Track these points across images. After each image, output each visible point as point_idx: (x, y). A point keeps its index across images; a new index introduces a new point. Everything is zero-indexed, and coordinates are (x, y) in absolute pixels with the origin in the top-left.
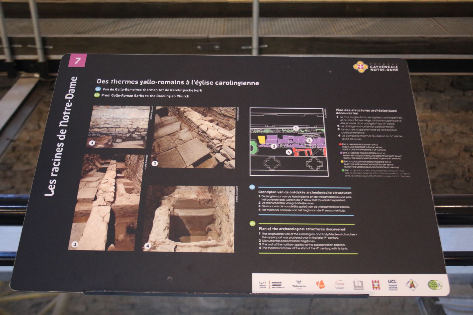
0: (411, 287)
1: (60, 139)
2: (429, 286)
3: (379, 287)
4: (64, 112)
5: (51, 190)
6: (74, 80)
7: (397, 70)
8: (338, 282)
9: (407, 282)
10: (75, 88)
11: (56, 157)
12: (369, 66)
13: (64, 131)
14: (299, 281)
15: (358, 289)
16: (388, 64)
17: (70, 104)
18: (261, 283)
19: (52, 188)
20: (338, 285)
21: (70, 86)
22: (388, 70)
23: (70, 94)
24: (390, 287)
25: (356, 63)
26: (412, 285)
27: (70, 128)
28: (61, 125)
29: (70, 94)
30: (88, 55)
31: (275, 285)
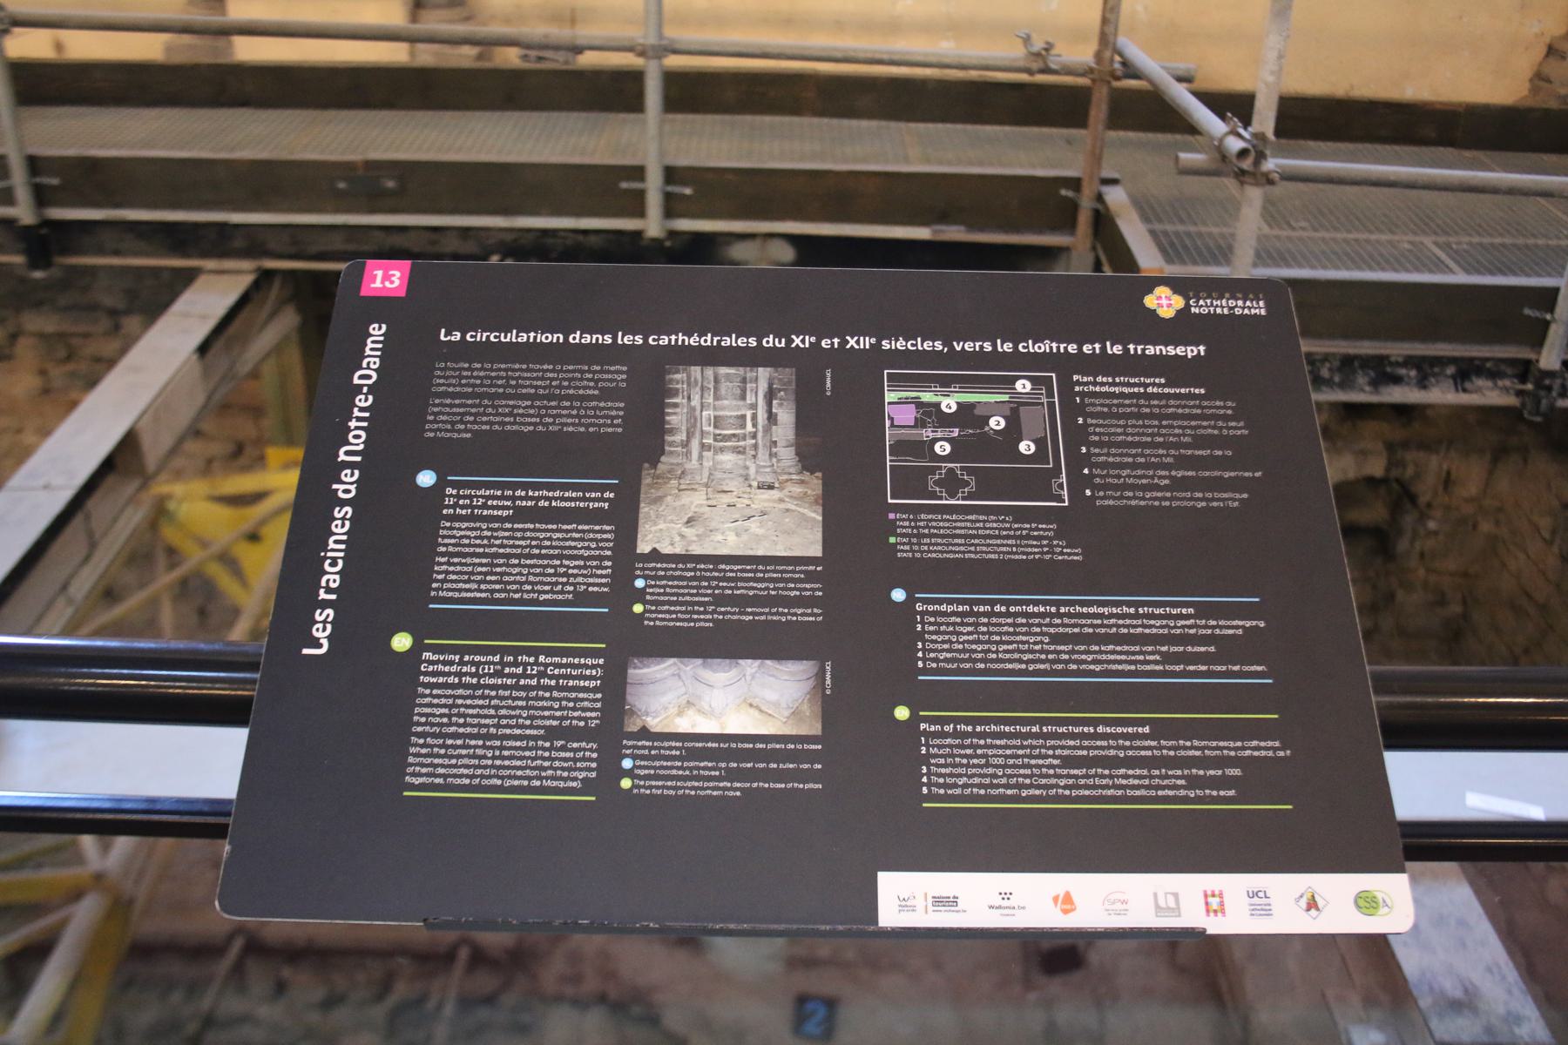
0: (1308, 909)
1: (341, 495)
4: (351, 421)
6: (377, 331)
8: (1112, 897)
10: (379, 353)
11: (332, 545)
14: (1006, 894)
15: (1166, 914)
17: (366, 400)
18: (901, 899)
19: (321, 633)
20: (1114, 903)
21: (367, 349)
24: (1253, 910)
26: (1312, 905)
28: (342, 457)
30: (413, 264)
31: (940, 904)
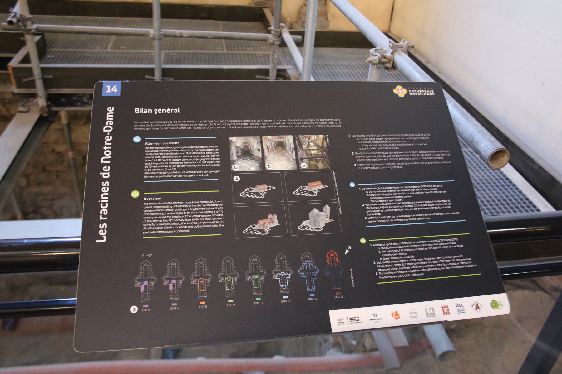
0: (476, 309)
1: (104, 177)
2: (492, 306)
3: (449, 312)
4: (104, 147)
5: (102, 236)
6: (111, 110)
7: (433, 94)
8: (412, 311)
9: (472, 304)
10: (112, 119)
11: (103, 198)
12: (408, 90)
13: (107, 168)
14: (375, 314)
16: (425, 88)
17: (109, 138)
19: (103, 233)
20: (412, 314)
22: (425, 94)
23: (109, 126)
24: (459, 311)
25: (395, 87)
26: (477, 307)
27: (113, 163)
28: (102, 162)
29: (109, 126)
